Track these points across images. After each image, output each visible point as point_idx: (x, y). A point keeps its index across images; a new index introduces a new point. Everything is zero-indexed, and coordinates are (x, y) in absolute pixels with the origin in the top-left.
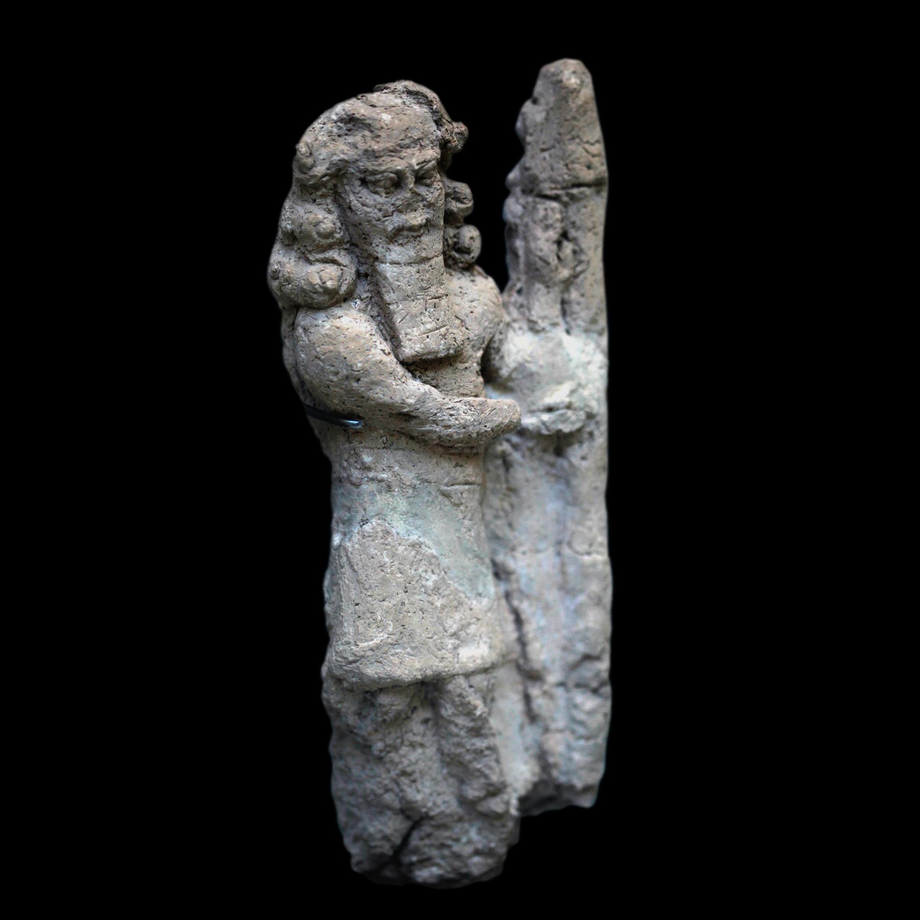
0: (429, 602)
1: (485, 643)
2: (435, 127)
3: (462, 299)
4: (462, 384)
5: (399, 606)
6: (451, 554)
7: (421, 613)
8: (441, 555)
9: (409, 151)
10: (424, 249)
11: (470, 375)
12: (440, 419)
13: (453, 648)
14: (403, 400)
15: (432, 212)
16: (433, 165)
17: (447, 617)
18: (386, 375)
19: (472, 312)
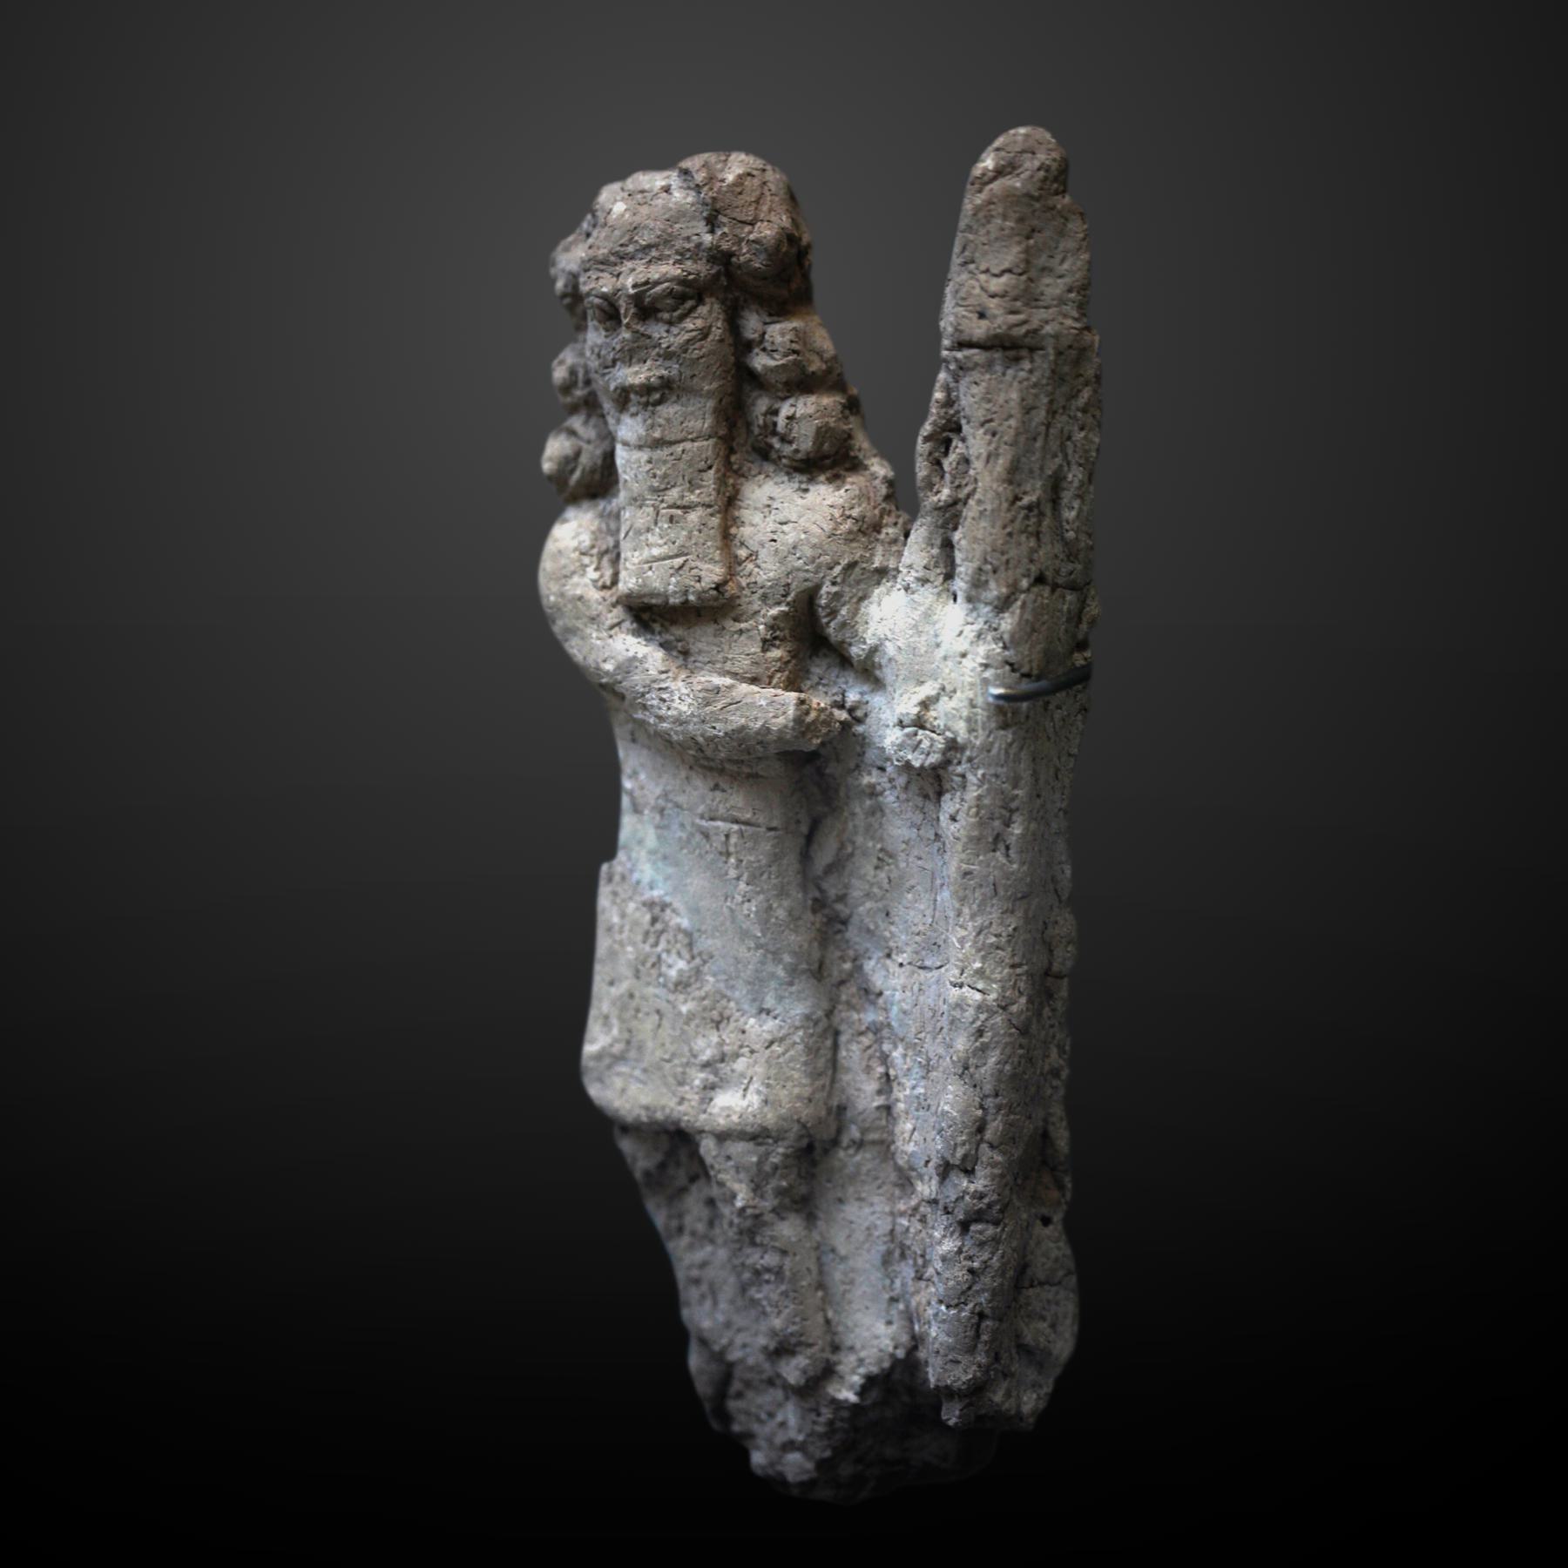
0: (668, 1001)
1: (758, 1092)
2: (701, 227)
3: (765, 517)
4: (730, 656)
5: (626, 999)
6: (717, 934)
7: (657, 1017)
8: (699, 930)
9: (629, 264)
10: (660, 426)
11: (749, 643)
12: (649, 703)
13: (702, 1086)
14: (597, 663)
15: (677, 366)
16: (664, 290)
17: (697, 1033)
18: (585, 620)
19: (775, 541)
